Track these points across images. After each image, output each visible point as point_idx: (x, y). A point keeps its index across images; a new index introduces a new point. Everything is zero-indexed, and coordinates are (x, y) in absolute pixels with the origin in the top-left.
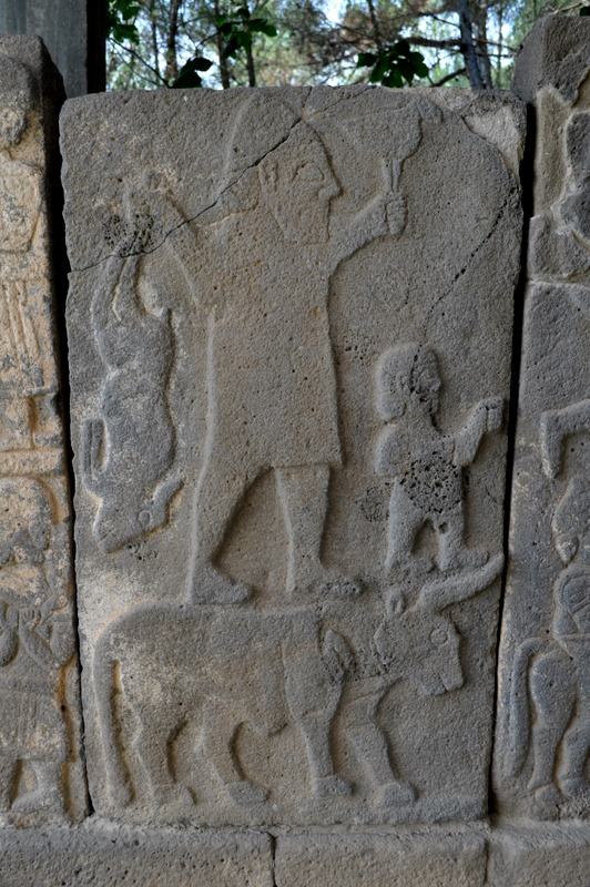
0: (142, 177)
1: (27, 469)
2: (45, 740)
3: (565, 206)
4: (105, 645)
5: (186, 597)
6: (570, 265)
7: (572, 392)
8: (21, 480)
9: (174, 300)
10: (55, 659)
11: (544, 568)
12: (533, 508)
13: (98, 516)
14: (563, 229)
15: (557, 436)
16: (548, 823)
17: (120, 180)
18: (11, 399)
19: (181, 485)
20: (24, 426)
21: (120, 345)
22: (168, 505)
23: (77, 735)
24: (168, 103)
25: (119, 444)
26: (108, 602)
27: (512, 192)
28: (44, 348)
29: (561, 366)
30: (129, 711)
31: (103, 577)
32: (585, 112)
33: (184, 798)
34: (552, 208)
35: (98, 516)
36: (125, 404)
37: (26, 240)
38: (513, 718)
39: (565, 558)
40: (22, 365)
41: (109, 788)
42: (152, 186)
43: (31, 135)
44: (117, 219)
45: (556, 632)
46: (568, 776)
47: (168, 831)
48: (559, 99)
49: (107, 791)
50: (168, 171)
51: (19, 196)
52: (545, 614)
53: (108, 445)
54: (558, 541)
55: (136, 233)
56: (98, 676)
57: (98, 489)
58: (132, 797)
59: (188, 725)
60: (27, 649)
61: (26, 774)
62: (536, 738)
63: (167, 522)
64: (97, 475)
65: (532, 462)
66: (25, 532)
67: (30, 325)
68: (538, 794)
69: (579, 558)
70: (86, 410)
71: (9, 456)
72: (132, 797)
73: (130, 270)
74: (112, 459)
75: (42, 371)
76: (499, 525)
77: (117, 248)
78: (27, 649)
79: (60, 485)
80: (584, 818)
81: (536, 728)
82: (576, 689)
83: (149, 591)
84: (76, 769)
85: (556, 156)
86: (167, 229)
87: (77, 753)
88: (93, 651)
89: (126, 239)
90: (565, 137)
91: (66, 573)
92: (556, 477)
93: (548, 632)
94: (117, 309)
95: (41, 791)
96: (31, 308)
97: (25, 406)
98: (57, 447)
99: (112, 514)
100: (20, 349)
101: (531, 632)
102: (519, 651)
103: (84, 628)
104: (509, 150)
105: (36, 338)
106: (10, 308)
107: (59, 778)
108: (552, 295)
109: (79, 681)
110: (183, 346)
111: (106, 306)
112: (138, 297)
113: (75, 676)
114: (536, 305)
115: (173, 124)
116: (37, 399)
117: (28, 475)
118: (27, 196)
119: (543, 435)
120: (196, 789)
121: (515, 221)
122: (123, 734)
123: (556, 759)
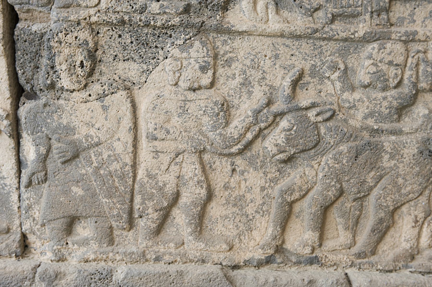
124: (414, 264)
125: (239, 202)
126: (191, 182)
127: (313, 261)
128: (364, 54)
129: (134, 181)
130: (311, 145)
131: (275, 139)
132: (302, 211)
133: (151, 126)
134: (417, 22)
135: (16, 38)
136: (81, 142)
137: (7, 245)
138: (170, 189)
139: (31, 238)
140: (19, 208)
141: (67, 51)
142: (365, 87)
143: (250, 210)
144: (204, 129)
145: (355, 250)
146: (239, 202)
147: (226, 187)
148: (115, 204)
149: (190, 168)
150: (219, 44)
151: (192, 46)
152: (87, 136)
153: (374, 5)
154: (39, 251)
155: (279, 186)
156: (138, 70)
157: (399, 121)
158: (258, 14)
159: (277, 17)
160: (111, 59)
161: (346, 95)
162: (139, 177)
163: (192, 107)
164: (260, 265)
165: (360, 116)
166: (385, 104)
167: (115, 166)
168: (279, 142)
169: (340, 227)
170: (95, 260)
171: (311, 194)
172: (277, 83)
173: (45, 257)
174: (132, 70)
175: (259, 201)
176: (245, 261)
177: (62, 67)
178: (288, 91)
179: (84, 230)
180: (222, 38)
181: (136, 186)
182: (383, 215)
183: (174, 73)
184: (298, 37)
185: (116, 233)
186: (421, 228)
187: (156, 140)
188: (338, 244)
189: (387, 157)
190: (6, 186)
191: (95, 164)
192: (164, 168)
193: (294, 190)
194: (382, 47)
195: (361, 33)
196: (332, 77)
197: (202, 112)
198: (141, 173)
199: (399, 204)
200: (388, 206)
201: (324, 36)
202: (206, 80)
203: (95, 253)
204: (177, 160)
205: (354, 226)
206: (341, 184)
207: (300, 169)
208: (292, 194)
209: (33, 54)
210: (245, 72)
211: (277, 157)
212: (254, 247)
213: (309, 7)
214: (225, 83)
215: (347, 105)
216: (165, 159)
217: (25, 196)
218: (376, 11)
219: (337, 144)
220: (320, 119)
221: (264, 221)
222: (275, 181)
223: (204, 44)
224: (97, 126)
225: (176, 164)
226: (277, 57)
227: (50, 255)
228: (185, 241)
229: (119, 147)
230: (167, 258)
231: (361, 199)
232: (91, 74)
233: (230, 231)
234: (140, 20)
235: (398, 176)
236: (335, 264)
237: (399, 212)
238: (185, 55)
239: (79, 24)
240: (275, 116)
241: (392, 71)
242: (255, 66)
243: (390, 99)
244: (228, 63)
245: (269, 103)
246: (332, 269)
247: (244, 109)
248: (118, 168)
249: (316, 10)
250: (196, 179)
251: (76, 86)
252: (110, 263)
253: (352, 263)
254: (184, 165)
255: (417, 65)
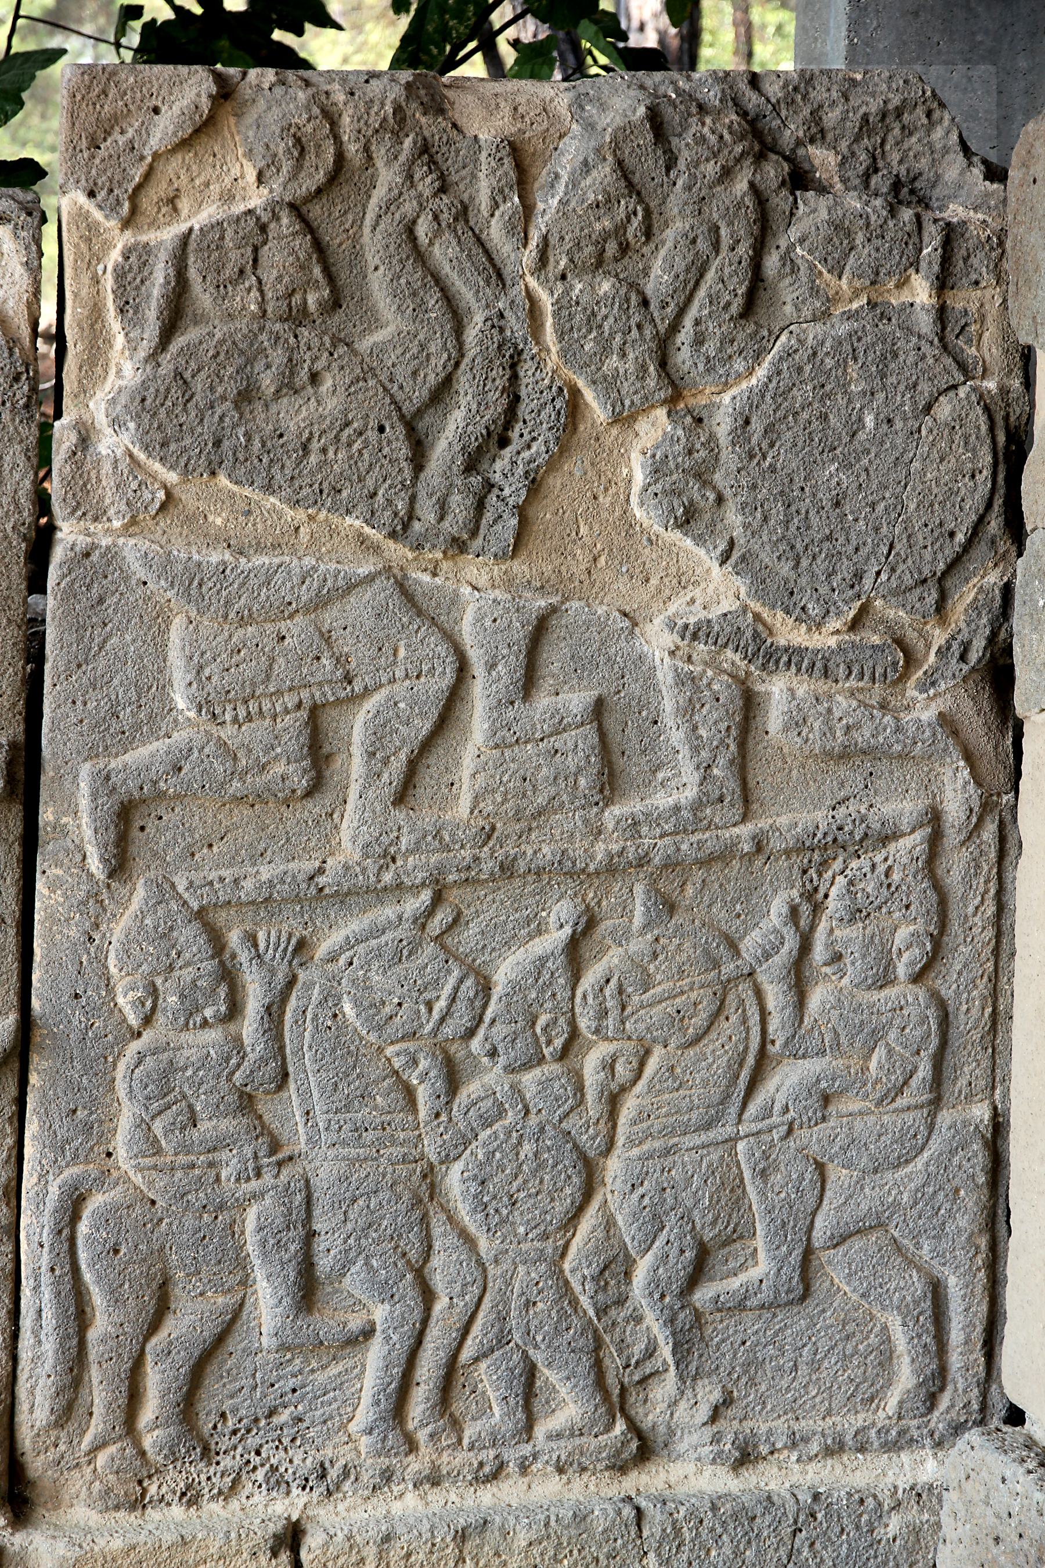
3: (113, 402)
6: (123, 507)
7: (137, 727)
11: (97, 1038)
12: (73, 932)
14: (111, 443)
15: (109, 805)
16: (121, 1514)
27: (17, 379)
29: (116, 682)
32: (144, 238)
34: (91, 405)
38: (47, 1314)
39: (133, 1020)
45: (121, 1153)
46: (156, 1425)
48: (98, 215)
52: (101, 1122)
54: (119, 990)
62: (94, 1352)
65: (67, 852)
68: (102, 1458)
69: (160, 1019)
76: (11, 963)
80: (190, 1504)
81: (93, 1335)
82: (165, 1261)
85: (96, 313)
90: (109, 282)
92: (110, 876)
93: (109, 1155)
101: (76, 1156)
102: (54, 1190)
104: (11, 303)
108: (95, 557)
114: (64, 576)
119: (84, 803)
121: (24, 431)
123: (134, 1397)
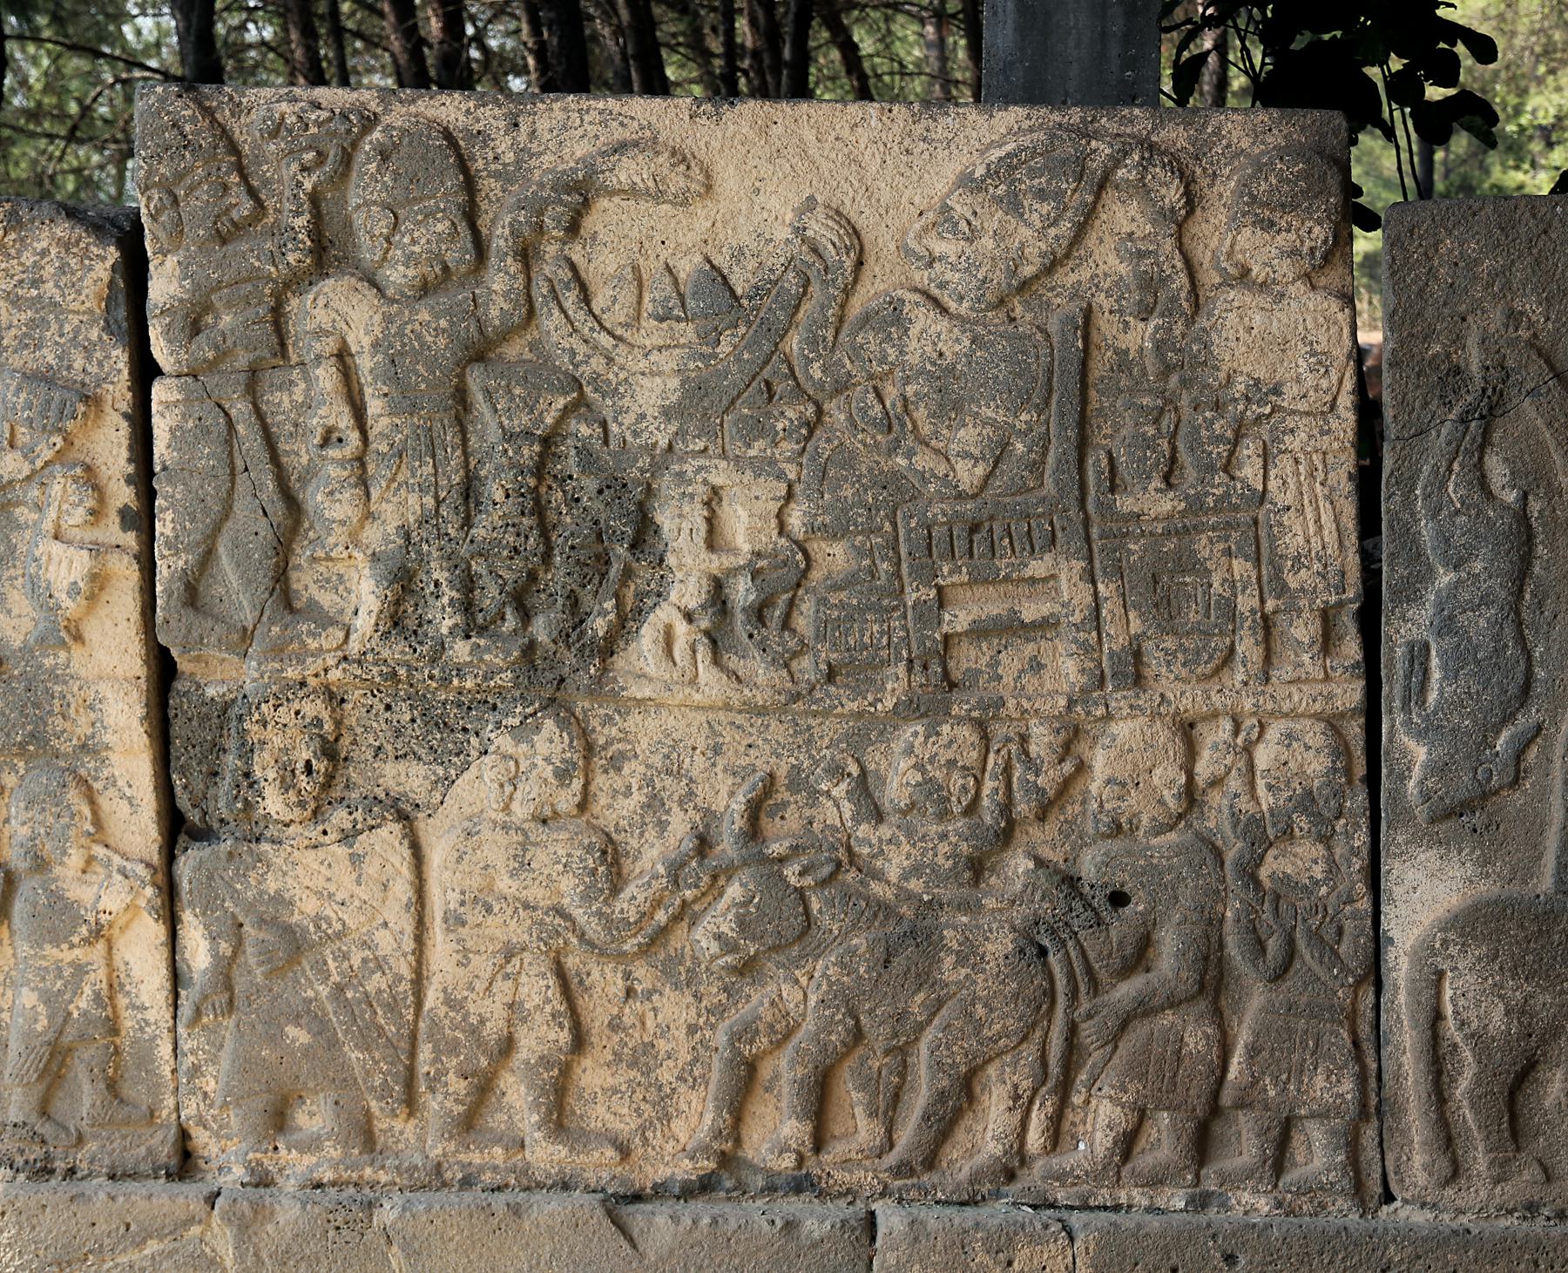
0: (1497, 316)
1: (1318, 707)
2: (1329, 1086)
4: (1426, 952)
5: (1545, 882)
8: (1308, 722)
9: (1533, 478)
10: (1350, 972)
13: (1417, 772)
17: (1464, 319)
18: (1300, 611)
19: (1539, 728)
20: (1316, 648)
21: (1459, 540)
22: (1519, 756)
23: (1373, 1083)
24: (1534, 216)
25: (1451, 674)
26: (1426, 893)
28: (1347, 543)
30: (1455, 1046)
31: (1422, 857)
33: (1531, 1173)
35: (1417, 772)
36: (1461, 619)
37: (1329, 398)
40: (1317, 566)
41: (1418, 1159)
42: (1511, 329)
43: (1338, 254)
44: (1457, 371)
47: (1504, 1223)
49: (1417, 1162)
50: (1531, 306)
51: (1323, 339)
53: (1436, 675)
55: (1484, 390)
56: (1414, 993)
57: (1420, 735)
58: (1455, 1173)
59: (1541, 1067)
60: (1308, 957)
61: (1297, 1139)
63: (1516, 782)
64: (1419, 715)
66: (1309, 793)
67: (1330, 513)
70: (1404, 629)
71: (1293, 689)
72: (1455, 1173)
73: (1474, 440)
74: (1441, 693)
75: (1343, 574)
77: (1457, 410)
78: (1308, 957)
79: (1358, 730)
83: (1488, 876)
84: (1369, 1133)
86: (1530, 385)
87: (1373, 1110)
88: (1404, 964)
89: (1469, 399)
91: (1365, 852)
94: (1455, 492)
95: (1319, 1161)
96: (1332, 489)
97: (1318, 622)
98: (1359, 677)
99: (1438, 769)
100: (1316, 544)
103: (1391, 923)
105: (1338, 530)
106: (1305, 489)
107: (1348, 1144)
109: (1377, 1007)
110: (1542, 542)
111: (1440, 489)
112: (1483, 476)
113: (1371, 998)
115: (1541, 244)
116: (1332, 612)
117: (1317, 717)
118: (1333, 340)
120: (1548, 1162)
122: (1445, 1079)
124: (1015, 1187)
125: (642, 1058)
126: (538, 1016)
127: (800, 1184)
128: (898, 747)
129: (417, 1014)
130: (789, 934)
131: (720, 919)
132: (776, 1077)
133: (454, 897)
134: (1005, 680)
135: (171, 713)
136: (305, 930)
137: (150, 1151)
138: (494, 1029)
139: (200, 1137)
140: (174, 1071)
141: (277, 741)
142: (904, 813)
143: (666, 1075)
144: (566, 901)
145: (891, 1159)
146: (642, 1058)
147: (615, 1025)
148: (377, 1063)
149: (537, 988)
150: (594, 723)
151: (538, 728)
152: (318, 919)
153: (914, 646)
154: (214, 1165)
155: (727, 1022)
156: (426, 778)
157: (977, 884)
158: (675, 664)
159: (714, 671)
160: (369, 755)
161: (863, 830)
162: (428, 1005)
163: (540, 858)
164: (688, 1192)
165: (893, 874)
166: (944, 848)
167: (376, 982)
168: (725, 928)
169: (859, 1110)
170: (333, 1184)
171: (795, 1040)
172: (719, 805)
173: (229, 1178)
174: (410, 778)
175: (685, 1056)
176: (655, 1186)
177: (264, 768)
178: (740, 823)
179: (313, 1117)
180: (602, 711)
181: (422, 1025)
182: (945, 1083)
183: (502, 786)
184: (762, 711)
185: (380, 1125)
186: (1028, 1111)
187: (463, 924)
188: (855, 1146)
189: (949, 961)
190: (148, 1024)
191: (335, 978)
192: (480, 986)
193: (757, 1032)
194: (932, 732)
195: (889, 703)
196: (834, 793)
197: (560, 867)
198: (432, 998)
199: (979, 1061)
200: (954, 1065)
201: (814, 707)
202: (566, 801)
203: (335, 1166)
204: (509, 969)
205: (889, 1109)
206: (858, 1021)
207: (771, 988)
208: (751, 1042)
209: (207, 746)
210: (650, 783)
211: (721, 962)
212: (674, 1155)
213: (780, 649)
214: (609, 806)
215: (866, 850)
216: (483, 965)
217: (186, 1046)
218: (918, 657)
219: (845, 934)
220: (808, 881)
221: (694, 1097)
222: (719, 1011)
223: (563, 725)
224: (339, 898)
225: (507, 977)
226: (717, 750)
227: (239, 1172)
228: (527, 1141)
229: (385, 942)
230: (487, 1177)
231: (901, 1054)
232: (327, 785)
233: (625, 1125)
234: (431, 677)
235: (975, 1000)
236: (849, 1191)
237: (981, 1077)
238: (524, 747)
239: (303, 684)
240: (715, 878)
241: (957, 781)
242: (674, 771)
243: (953, 839)
244: (616, 763)
245: (704, 844)
246: (842, 1203)
247: (650, 856)
248: (384, 986)
249: (795, 655)
250: (548, 1009)
251: (296, 814)
252: (367, 1190)
253: (886, 1187)
254: (523, 979)
255: (1007, 770)
